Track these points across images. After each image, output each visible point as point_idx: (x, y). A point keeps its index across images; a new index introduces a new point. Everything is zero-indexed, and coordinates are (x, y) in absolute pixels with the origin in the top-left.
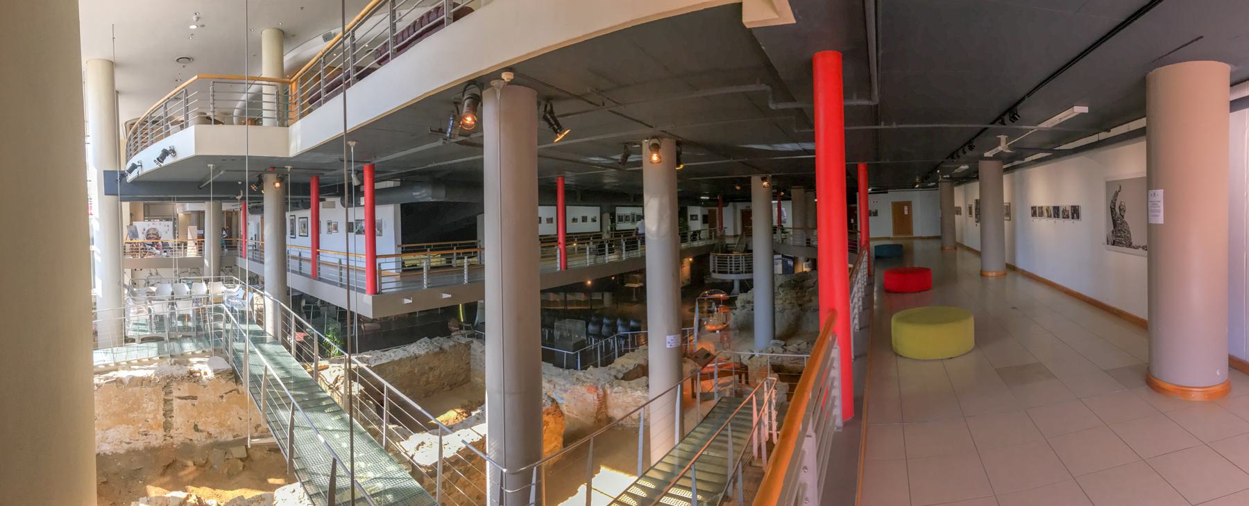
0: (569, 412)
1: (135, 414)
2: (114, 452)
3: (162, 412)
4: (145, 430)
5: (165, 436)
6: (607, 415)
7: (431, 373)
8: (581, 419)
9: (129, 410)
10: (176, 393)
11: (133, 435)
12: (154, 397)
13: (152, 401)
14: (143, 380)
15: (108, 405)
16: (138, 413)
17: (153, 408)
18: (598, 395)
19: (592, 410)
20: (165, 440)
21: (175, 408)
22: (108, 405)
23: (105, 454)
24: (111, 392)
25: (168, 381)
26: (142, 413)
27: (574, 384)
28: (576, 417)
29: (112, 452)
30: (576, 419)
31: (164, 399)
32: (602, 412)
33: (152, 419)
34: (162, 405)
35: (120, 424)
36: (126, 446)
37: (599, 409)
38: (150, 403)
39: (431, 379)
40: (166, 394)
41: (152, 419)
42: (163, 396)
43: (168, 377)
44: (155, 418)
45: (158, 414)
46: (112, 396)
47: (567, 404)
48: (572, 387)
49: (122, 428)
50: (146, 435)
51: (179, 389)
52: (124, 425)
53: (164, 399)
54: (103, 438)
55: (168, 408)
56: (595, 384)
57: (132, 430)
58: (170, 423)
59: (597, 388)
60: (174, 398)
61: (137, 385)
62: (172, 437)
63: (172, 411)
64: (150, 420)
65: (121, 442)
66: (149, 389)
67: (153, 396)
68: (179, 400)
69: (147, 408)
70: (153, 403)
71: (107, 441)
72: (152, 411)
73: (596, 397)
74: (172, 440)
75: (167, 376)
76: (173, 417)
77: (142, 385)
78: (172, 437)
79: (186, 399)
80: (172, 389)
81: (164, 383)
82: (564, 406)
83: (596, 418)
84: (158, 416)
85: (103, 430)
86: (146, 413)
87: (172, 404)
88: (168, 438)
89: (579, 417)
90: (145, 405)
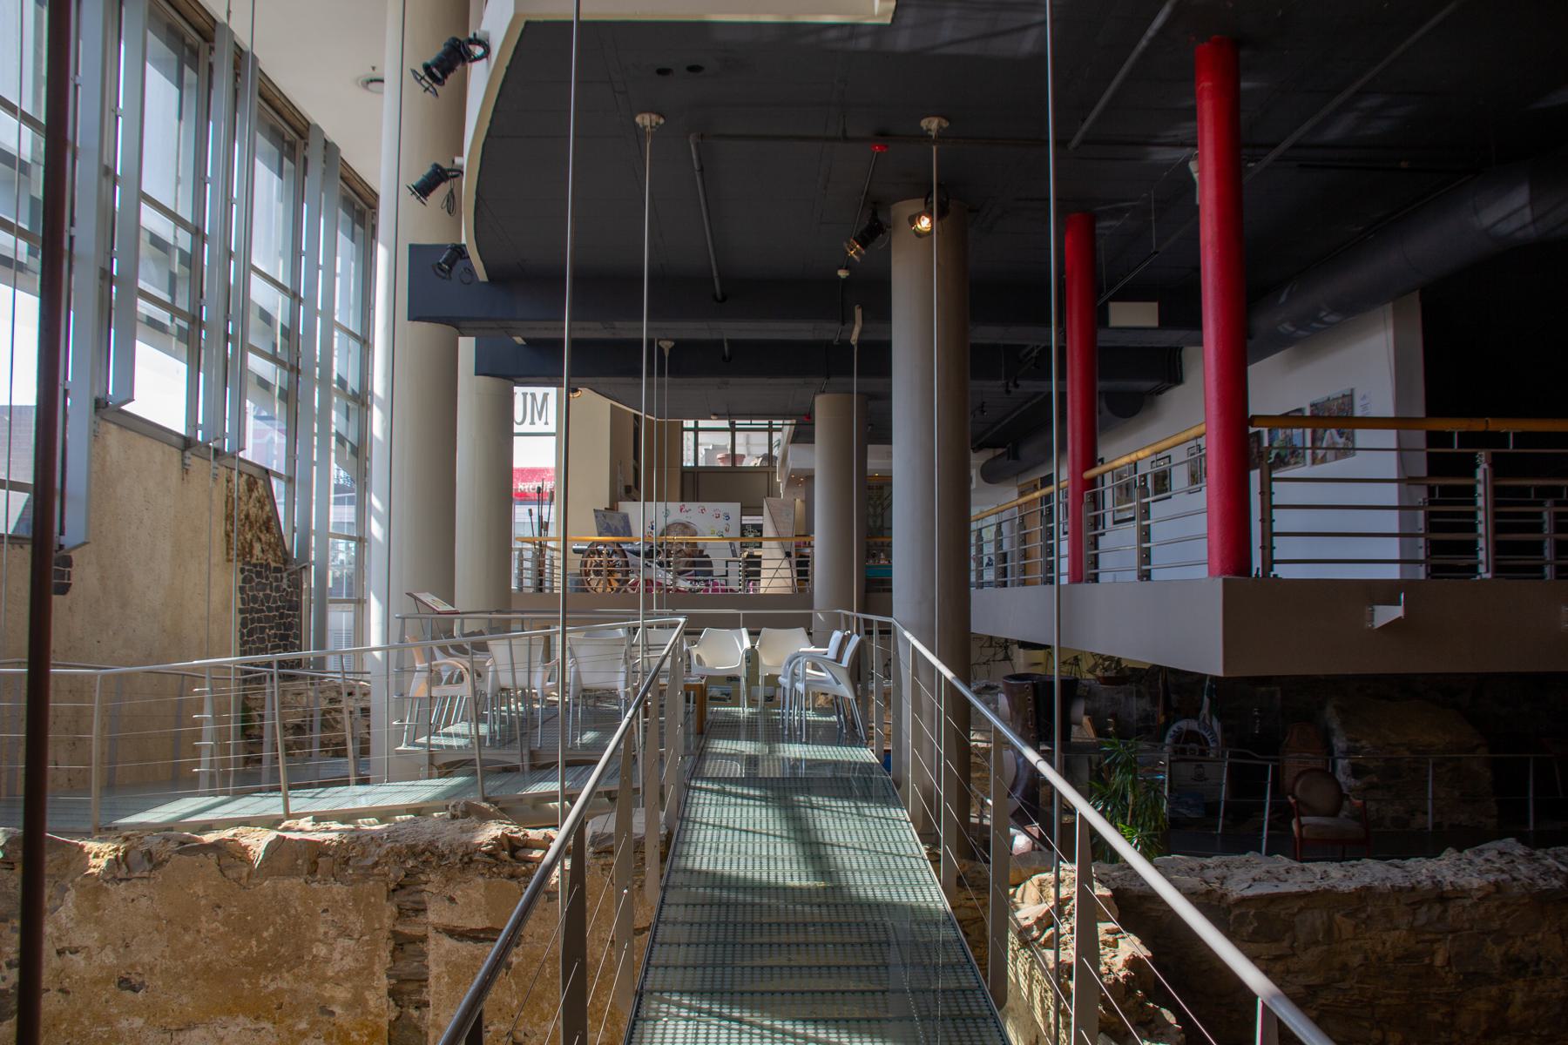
1: (285, 982)
3: (383, 983)
9: (261, 964)
10: (437, 914)
12: (356, 922)
13: (350, 937)
14: (319, 855)
15: (188, 938)
16: (296, 978)
17: (349, 962)
21: (434, 970)
22: (188, 938)
25: (410, 863)
26: (310, 977)
31: (395, 934)
33: (349, 1006)
34: (385, 955)
40: (402, 914)
41: (349, 1006)
42: (388, 922)
43: (413, 851)
44: (357, 1002)
45: (370, 987)
46: (203, 902)
51: (452, 900)
53: (395, 934)
55: (408, 967)
58: (417, 1029)
60: (431, 933)
61: (292, 871)
63: (422, 981)
64: (338, 1010)
66: (340, 891)
67: (352, 918)
68: (448, 943)
69: (327, 960)
70: (347, 942)
72: (349, 975)
75: (411, 848)
76: (426, 1004)
77: (312, 872)
79: (476, 939)
80: (425, 896)
81: (395, 873)
86: (325, 979)
87: (424, 954)
90: (321, 950)
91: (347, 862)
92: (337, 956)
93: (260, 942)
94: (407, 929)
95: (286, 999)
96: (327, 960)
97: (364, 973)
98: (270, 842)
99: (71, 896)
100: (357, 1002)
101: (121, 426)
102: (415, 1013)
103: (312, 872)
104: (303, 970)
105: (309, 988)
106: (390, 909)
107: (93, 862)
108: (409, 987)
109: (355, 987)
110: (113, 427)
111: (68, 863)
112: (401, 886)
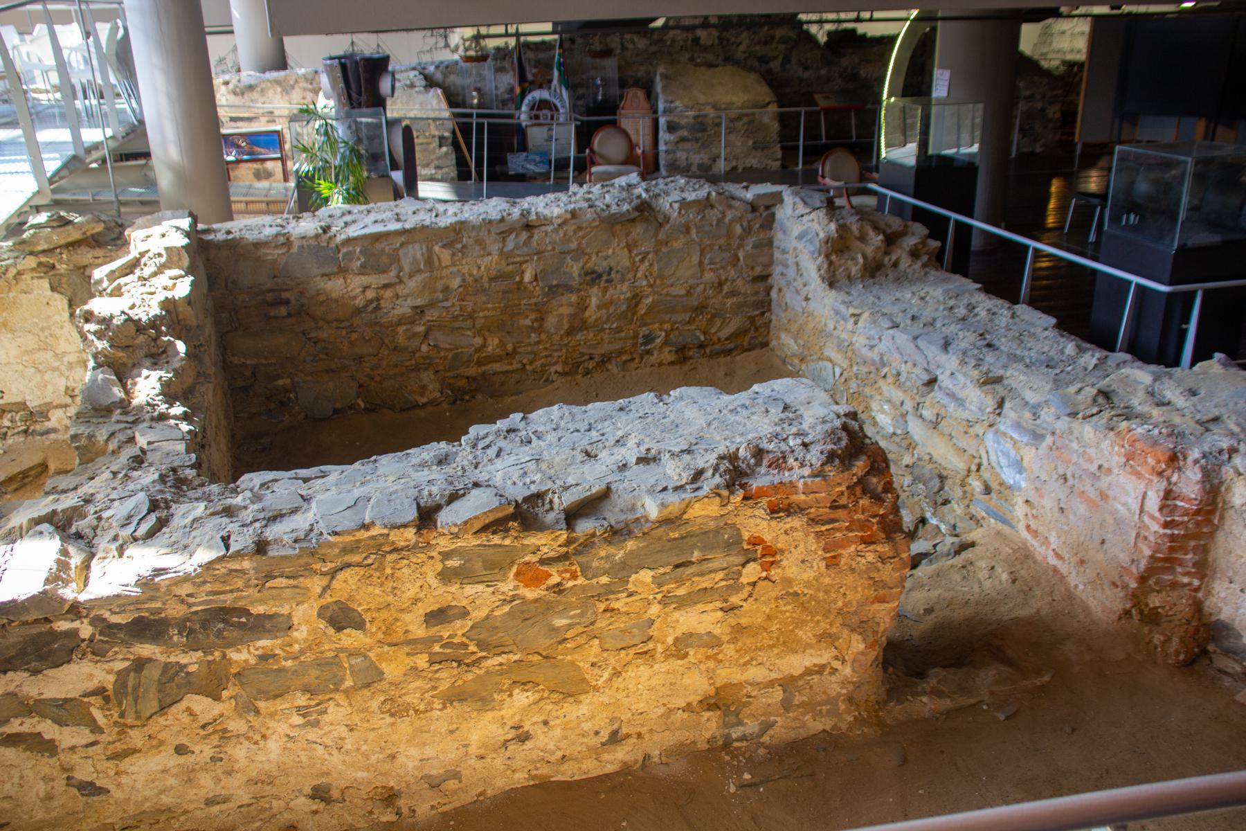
0: (1035, 533)
6: (1198, 606)
7: (595, 290)
8: (1073, 580)
18: (1168, 494)
19: (1124, 558)
27: (1073, 415)
28: (1053, 561)
30: (1055, 570)
32: (1174, 585)
37: (1162, 563)
39: (591, 314)
47: (1032, 496)
48: (1062, 424)
56: (1175, 433)
59: (1174, 459)
73: (1153, 502)
82: (1020, 501)
83: (1137, 598)
89: (1064, 569)
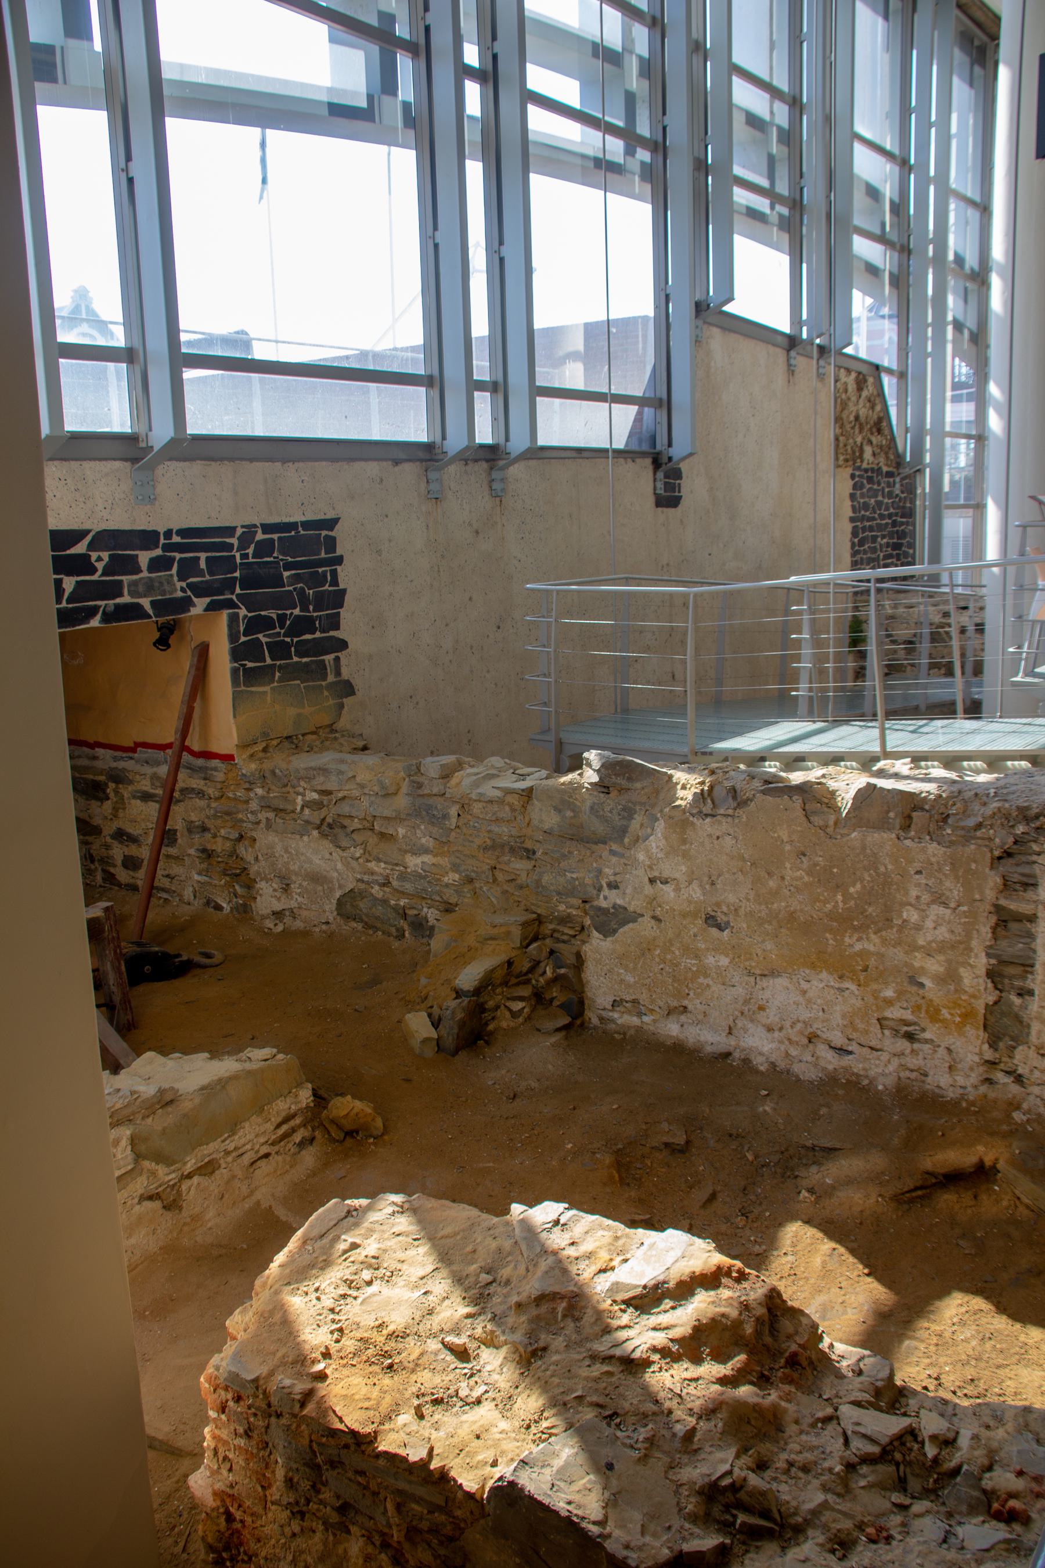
1: (871, 943)
2: (782, 1065)
3: (982, 962)
4: (908, 1015)
5: (992, 1064)
11: (861, 1026)
12: (954, 890)
13: (945, 905)
14: (914, 809)
16: (884, 941)
17: (943, 933)
20: (988, 1081)
23: (746, 1061)
24: (784, 835)
25: (1020, 829)
26: (898, 943)
29: (773, 1065)
31: (998, 909)
33: (941, 980)
34: (986, 931)
35: (813, 966)
36: (830, 1060)
38: (937, 910)
40: (1007, 885)
41: (941, 980)
42: (990, 894)
44: (950, 977)
45: (966, 964)
46: (788, 848)
49: (821, 983)
50: (910, 1037)
52: (824, 975)
53: (998, 909)
54: (747, 1002)
55: (1012, 948)
57: (859, 1004)
58: (1018, 1019)
61: (883, 825)
62: (1019, 1079)
64: (928, 983)
65: (812, 1038)
66: (934, 850)
67: (948, 884)
69: (918, 928)
70: (942, 910)
71: (761, 1016)
72: (942, 947)
74: (1015, 1089)
76: (1031, 993)
77: (906, 827)
78: (1019, 1079)
80: (1037, 870)
81: (1002, 839)
84: (963, 971)
85: (750, 974)
86: (914, 948)
87: (1031, 936)
88: (1001, 1077)
90: (912, 916)
91: (945, 819)
92: (929, 924)
93: (847, 897)
94: (1013, 906)
95: (872, 962)
96: (918, 928)
97: (961, 946)
98: (860, 790)
99: (660, 826)
100: (950, 977)
101: (724, 329)
102: (1017, 1001)
103: (906, 827)
104: (892, 934)
105: (897, 955)
106: (994, 879)
107: (681, 793)
108: (1011, 970)
109: (949, 961)
110: (716, 331)
111: (657, 792)
112: (1008, 854)
